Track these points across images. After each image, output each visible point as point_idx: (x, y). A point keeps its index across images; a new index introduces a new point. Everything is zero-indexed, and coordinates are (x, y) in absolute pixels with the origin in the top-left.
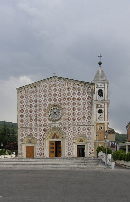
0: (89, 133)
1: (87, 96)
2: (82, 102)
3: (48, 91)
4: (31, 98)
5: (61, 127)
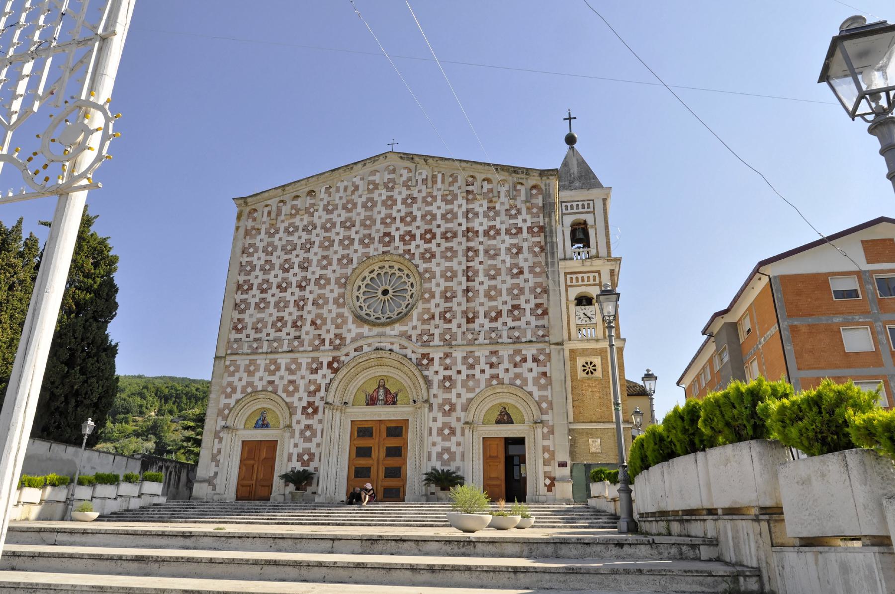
0: (543, 381)
1: (525, 221)
2: (503, 247)
3: (359, 205)
4: (290, 233)
5: (409, 352)
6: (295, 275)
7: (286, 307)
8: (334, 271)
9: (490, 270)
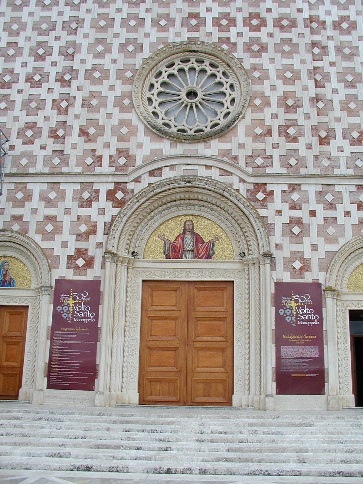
5: (234, 180)
6: (54, 64)
7: (39, 109)
8: (115, 61)
9: (346, 74)
